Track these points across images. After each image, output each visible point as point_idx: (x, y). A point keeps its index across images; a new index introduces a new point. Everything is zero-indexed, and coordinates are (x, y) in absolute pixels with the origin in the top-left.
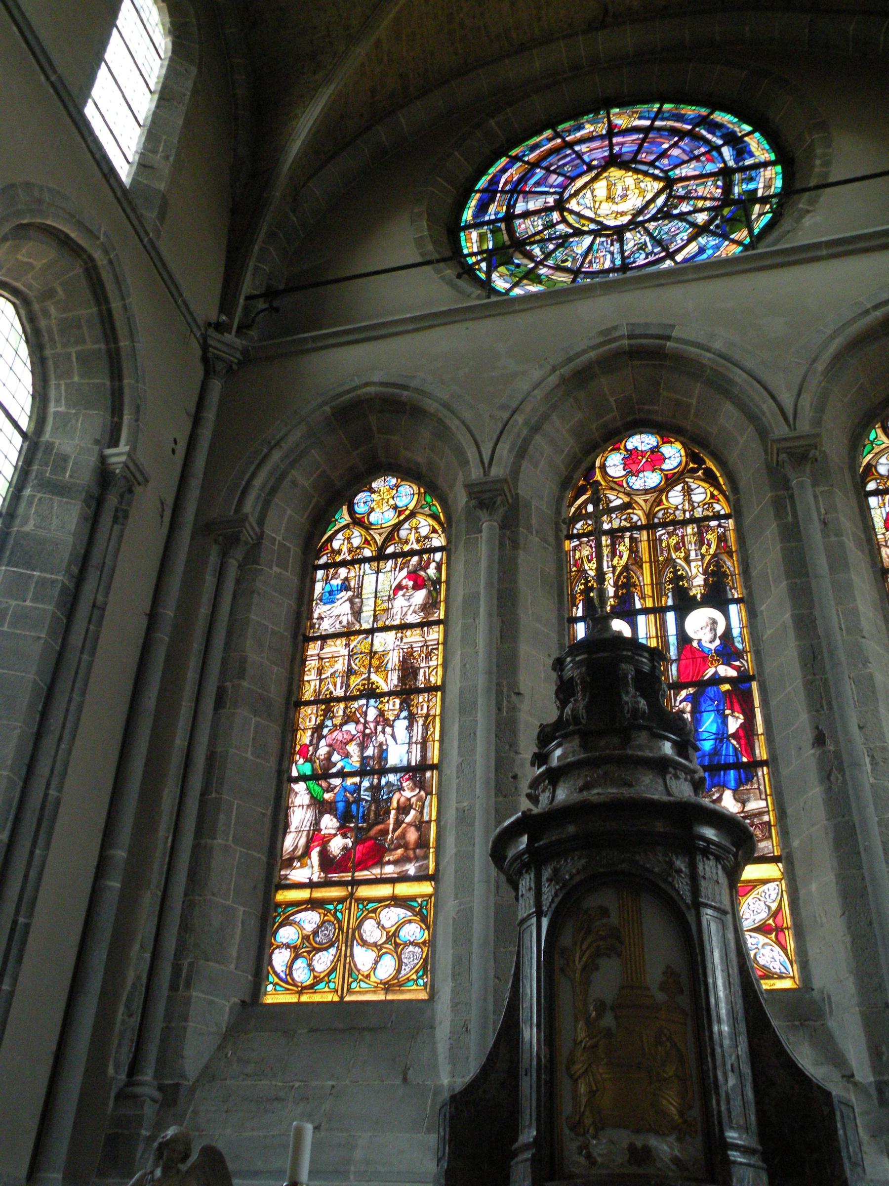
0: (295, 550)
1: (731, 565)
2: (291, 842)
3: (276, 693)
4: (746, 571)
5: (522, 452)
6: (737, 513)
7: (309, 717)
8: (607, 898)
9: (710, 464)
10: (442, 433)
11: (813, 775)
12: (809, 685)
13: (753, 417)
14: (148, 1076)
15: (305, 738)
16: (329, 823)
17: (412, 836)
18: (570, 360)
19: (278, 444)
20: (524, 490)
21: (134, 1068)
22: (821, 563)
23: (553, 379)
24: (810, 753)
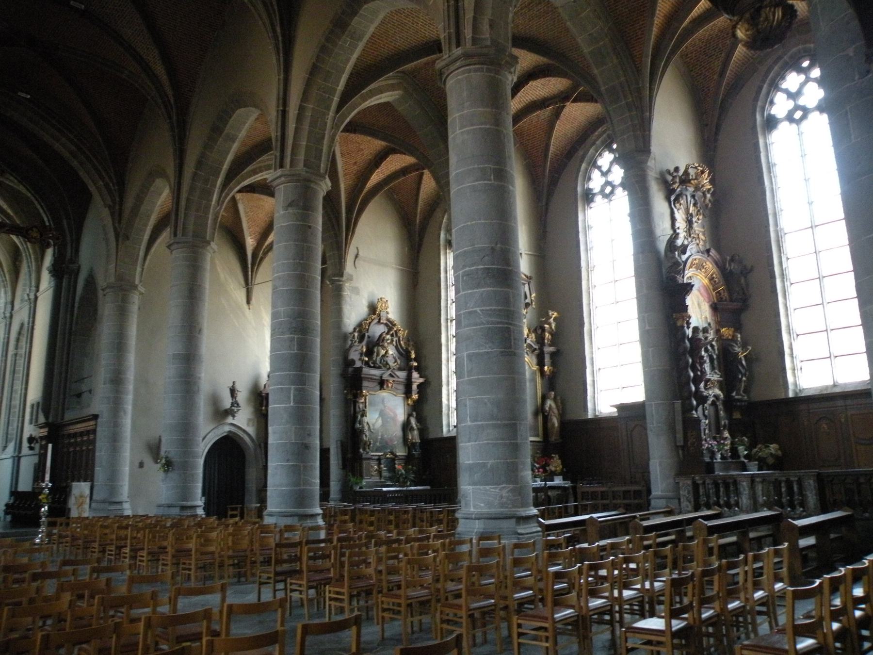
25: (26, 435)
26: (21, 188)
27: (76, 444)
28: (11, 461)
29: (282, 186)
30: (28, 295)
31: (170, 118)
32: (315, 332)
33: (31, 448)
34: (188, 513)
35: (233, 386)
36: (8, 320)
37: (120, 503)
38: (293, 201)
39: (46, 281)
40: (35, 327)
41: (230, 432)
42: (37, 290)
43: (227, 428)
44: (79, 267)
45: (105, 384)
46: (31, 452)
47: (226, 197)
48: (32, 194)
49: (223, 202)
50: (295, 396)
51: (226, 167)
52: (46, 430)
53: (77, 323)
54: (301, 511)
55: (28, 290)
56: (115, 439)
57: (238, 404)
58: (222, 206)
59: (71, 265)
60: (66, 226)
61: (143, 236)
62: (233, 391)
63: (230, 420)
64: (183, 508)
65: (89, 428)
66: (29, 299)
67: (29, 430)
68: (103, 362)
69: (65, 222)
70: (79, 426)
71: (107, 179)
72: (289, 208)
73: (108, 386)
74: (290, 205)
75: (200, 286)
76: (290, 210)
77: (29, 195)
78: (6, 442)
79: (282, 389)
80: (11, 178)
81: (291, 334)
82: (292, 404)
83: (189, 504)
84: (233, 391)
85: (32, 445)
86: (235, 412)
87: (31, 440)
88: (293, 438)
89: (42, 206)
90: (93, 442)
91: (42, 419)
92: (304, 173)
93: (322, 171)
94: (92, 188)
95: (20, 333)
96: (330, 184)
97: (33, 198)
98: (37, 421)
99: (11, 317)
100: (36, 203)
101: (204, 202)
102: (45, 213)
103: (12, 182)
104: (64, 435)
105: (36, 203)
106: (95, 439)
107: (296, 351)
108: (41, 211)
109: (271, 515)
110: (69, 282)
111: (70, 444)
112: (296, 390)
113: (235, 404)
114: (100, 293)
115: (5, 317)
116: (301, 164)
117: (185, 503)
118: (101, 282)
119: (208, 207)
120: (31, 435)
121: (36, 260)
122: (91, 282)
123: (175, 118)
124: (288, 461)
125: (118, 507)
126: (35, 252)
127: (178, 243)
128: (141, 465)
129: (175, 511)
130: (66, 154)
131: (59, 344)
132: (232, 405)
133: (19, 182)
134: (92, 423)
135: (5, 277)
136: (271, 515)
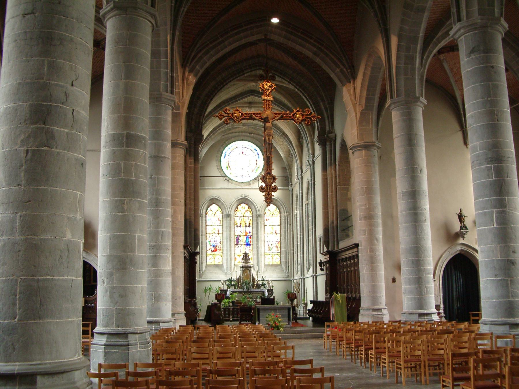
0: (205, 214)
1: (251, 223)
2: (208, 249)
3: (205, 233)
4: (252, 224)
5: (231, 209)
6: (252, 217)
7: (208, 235)
8: (246, 270)
9: (250, 209)
10: (222, 204)
11: (256, 248)
12: (257, 240)
13: (255, 209)
14: (201, 271)
15: (208, 237)
16: (212, 247)
17: (220, 249)
18: (238, 198)
19: (204, 203)
20: (232, 214)
21: (200, 271)
22: (259, 227)
23: (236, 200)
24: (256, 246)
25: (318, 261)
26: (291, 87)
27: (347, 266)
28: (312, 278)
29: (463, 37)
30: (308, 161)
31: (373, 7)
32: (510, 159)
33: (322, 270)
34: (425, 319)
35: (460, 213)
36: (300, 181)
37: (380, 310)
38: (474, 48)
39: (318, 149)
40: (315, 183)
41: (461, 250)
42: (314, 157)
43: (459, 248)
44: (336, 135)
45: (360, 220)
46: (323, 272)
47: (427, 59)
48: (298, 90)
49: (426, 63)
50: (497, 218)
51: (421, 34)
52: (328, 256)
53: (339, 176)
54: (511, 320)
55: (308, 157)
56: (372, 260)
57: (466, 228)
58: (425, 67)
59: (330, 135)
60: (323, 107)
61: (374, 104)
62: (461, 217)
63: (461, 241)
64: (421, 315)
65: (354, 254)
66: (309, 164)
67: (321, 258)
68: (358, 204)
69: (321, 104)
70: (347, 252)
71: (341, 66)
72: (472, 55)
73: (363, 221)
74: (472, 52)
75: (416, 134)
76: (473, 56)
77: (296, 90)
78: (309, 266)
79: (485, 213)
80: (284, 81)
81: (488, 163)
82: (495, 226)
83: (426, 311)
84: (461, 217)
85: (323, 267)
86: (464, 234)
87: (321, 264)
88: (499, 256)
89: (305, 97)
90: (357, 264)
91: (326, 250)
92: (479, 21)
93: (497, 15)
94: (333, 75)
95: (308, 189)
96: (506, 25)
97: (299, 92)
98: (321, 252)
99: (302, 178)
100: (301, 95)
101: (409, 66)
102: (308, 101)
103: (285, 83)
104: (339, 260)
105: (301, 95)
106: (358, 261)
107: (494, 179)
108: (306, 100)
109: (485, 324)
110: (331, 147)
111: (344, 267)
112: (497, 212)
113: (464, 227)
114: (350, 152)
115: (298, 179)
116: (476, 14)
117: (422, 311)
118: (350, 143)
119: (413, 69)
120: (321, 260)
121: (310, 136)
122: (344, 145)
123: (376, 7)
124: (496, 276)
125: (379, 313)
126: (309, 130)
127: (394, 103)
128: (394, 280)
129: (416, 318)
130: (310, 54)
131: (329, 194)
132: (461, 228)
133: (289, 82)
134: (355, 250)
135: (295, 151)
136: (485, 324)
